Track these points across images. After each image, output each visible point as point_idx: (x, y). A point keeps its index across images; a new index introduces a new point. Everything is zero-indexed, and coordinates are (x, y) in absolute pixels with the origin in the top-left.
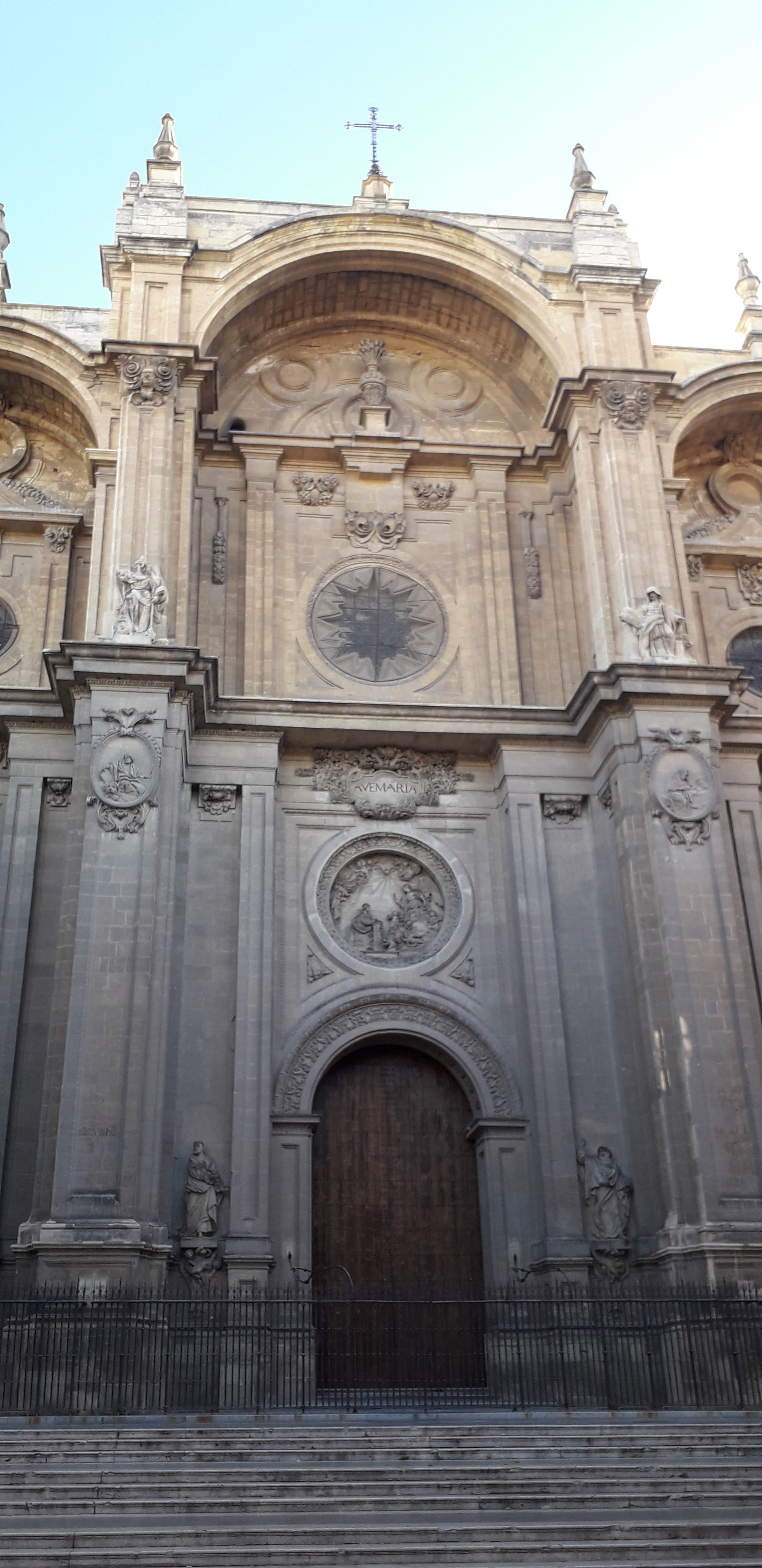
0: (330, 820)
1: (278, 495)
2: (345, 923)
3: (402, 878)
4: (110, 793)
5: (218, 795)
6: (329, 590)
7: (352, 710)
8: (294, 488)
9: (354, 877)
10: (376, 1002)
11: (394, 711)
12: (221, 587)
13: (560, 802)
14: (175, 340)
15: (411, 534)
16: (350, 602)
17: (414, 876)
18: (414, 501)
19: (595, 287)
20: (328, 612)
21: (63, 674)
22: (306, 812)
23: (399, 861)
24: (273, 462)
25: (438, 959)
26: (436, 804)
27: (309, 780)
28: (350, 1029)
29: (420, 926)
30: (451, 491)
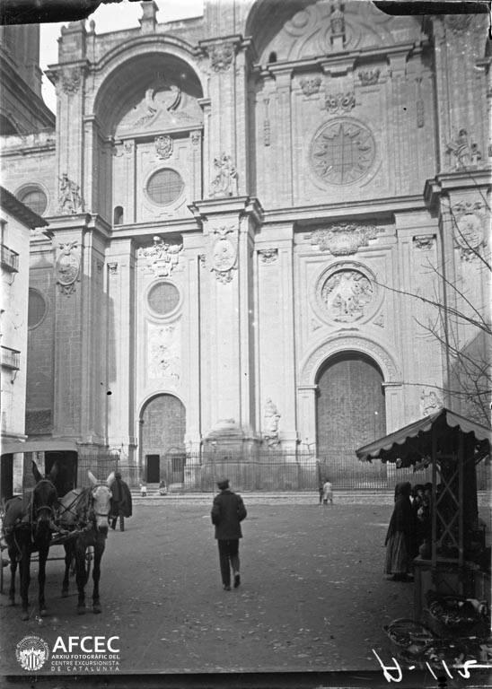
1: (293, 93)
2: (330, 303)
3: (355, 280)
4: (219, 266)
5: (268, 254)
6: (319, 139)
8: (300, 87)
12: (269, 147)
14: (232, 34)
15: (357, 102)
16: (329, 144)
18: (360, 83)
20: (318, 151)
21: (197, 214)
24: (289, 76)
26: (367, 245)
30: (378, 73)
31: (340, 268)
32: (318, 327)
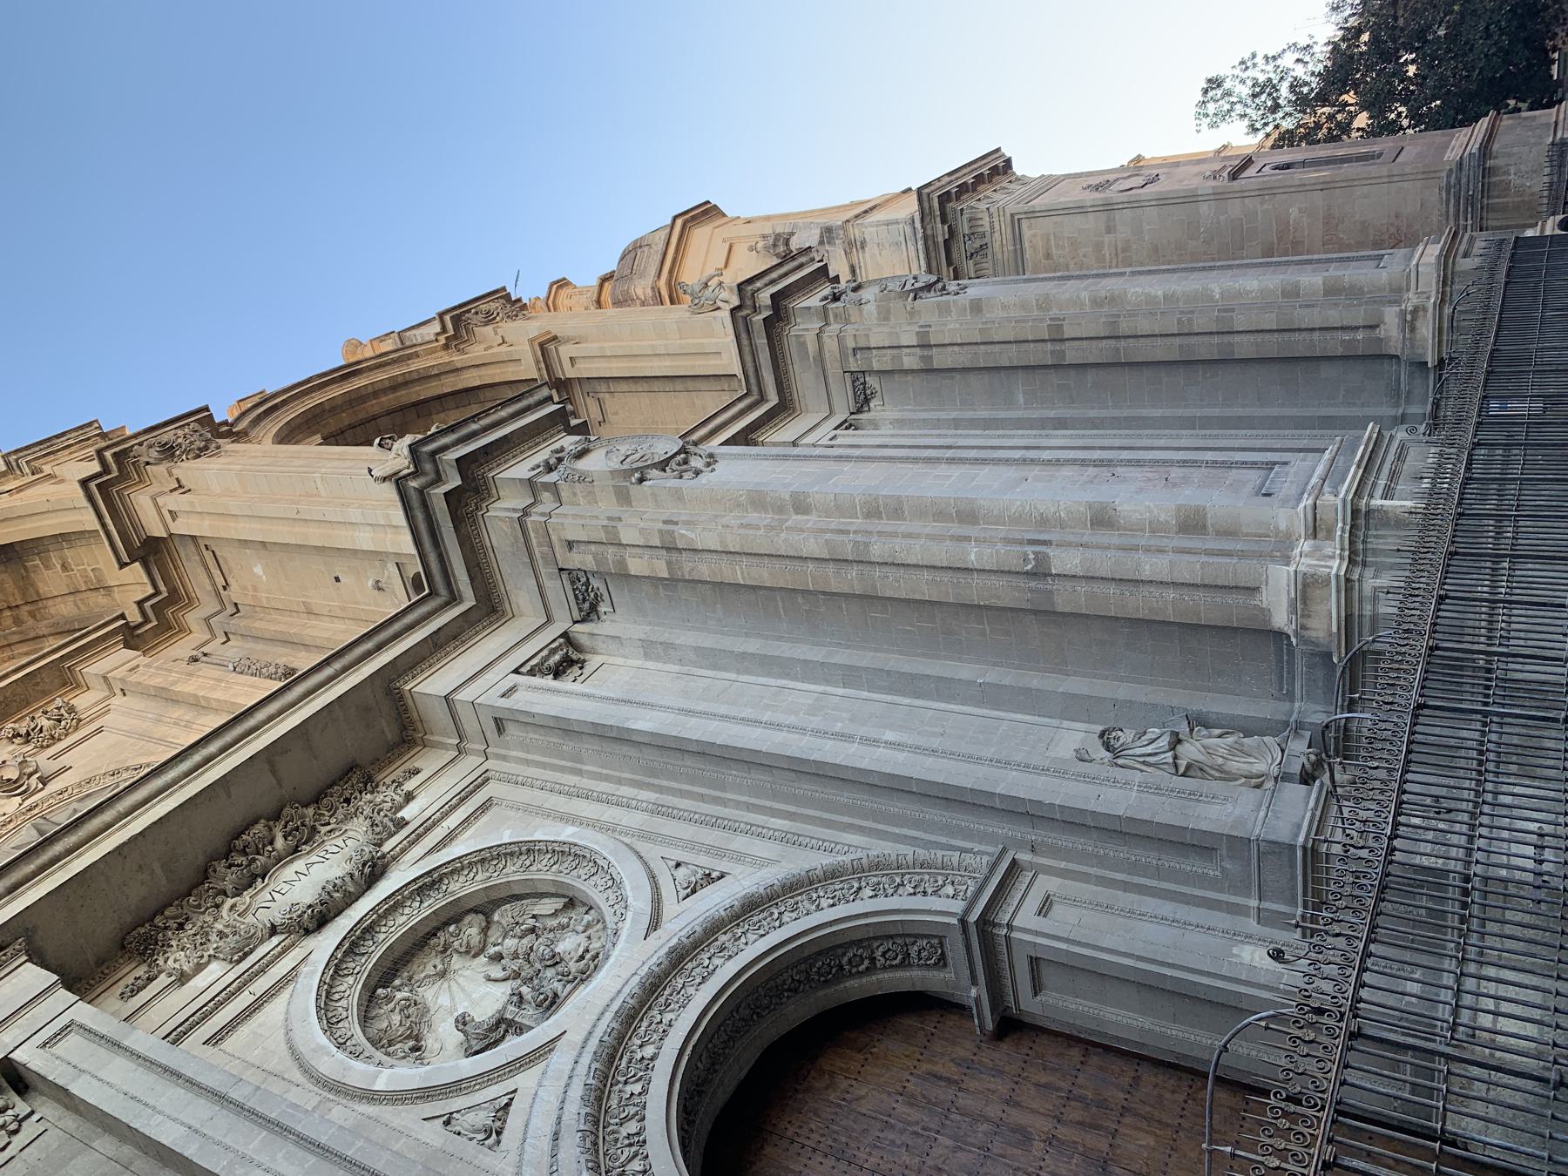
0: (261, 985)
3: (472, 952)
7: (121, 806)
9: (396, 1018)
10: (634, 1018)
11: (197, 758)
13: (546, 658)
17: (485, 931)
19: (52, 457)
22: (204, 1014)
23: (443, 936)
25: (640, 903)
26: (402, 824)
27: (163, 980)
28: (644, 1091)
29: (568, 945)
31: (375, 951)
32: (508, 1105)
